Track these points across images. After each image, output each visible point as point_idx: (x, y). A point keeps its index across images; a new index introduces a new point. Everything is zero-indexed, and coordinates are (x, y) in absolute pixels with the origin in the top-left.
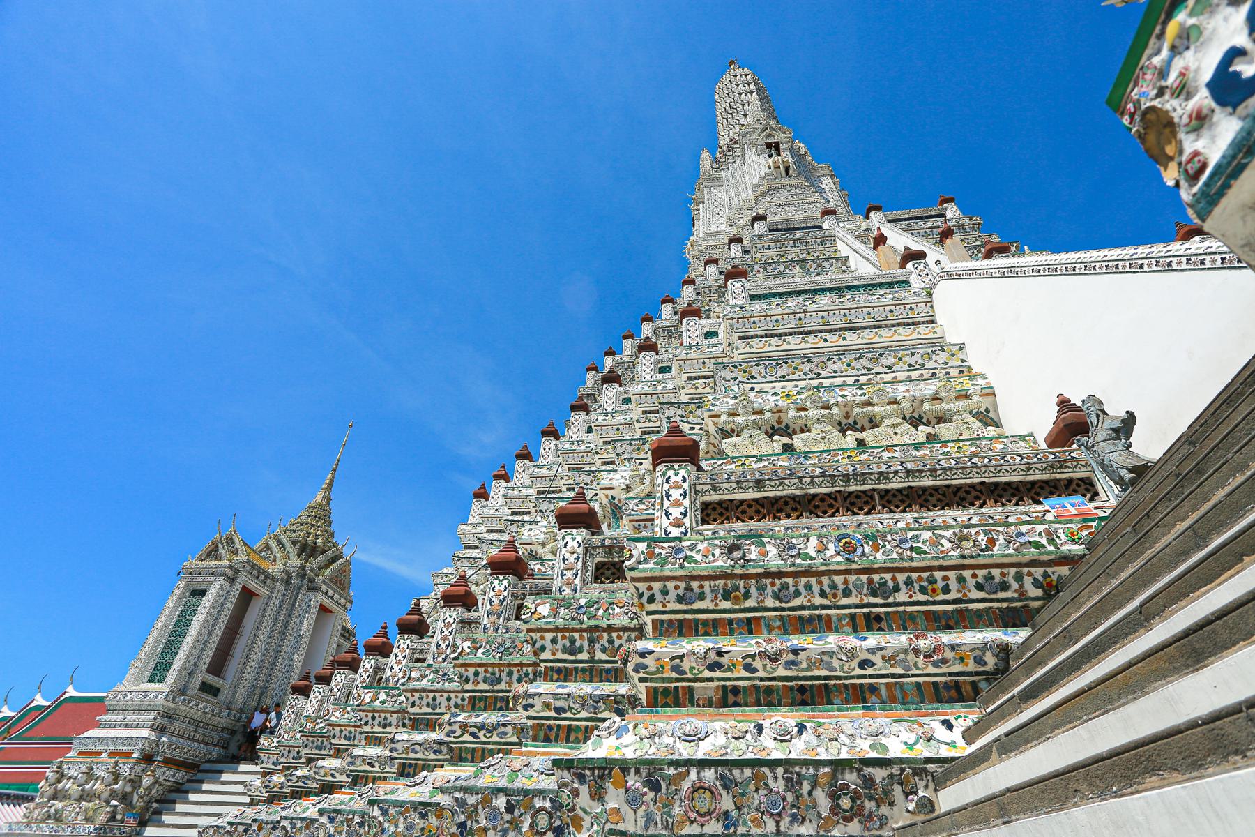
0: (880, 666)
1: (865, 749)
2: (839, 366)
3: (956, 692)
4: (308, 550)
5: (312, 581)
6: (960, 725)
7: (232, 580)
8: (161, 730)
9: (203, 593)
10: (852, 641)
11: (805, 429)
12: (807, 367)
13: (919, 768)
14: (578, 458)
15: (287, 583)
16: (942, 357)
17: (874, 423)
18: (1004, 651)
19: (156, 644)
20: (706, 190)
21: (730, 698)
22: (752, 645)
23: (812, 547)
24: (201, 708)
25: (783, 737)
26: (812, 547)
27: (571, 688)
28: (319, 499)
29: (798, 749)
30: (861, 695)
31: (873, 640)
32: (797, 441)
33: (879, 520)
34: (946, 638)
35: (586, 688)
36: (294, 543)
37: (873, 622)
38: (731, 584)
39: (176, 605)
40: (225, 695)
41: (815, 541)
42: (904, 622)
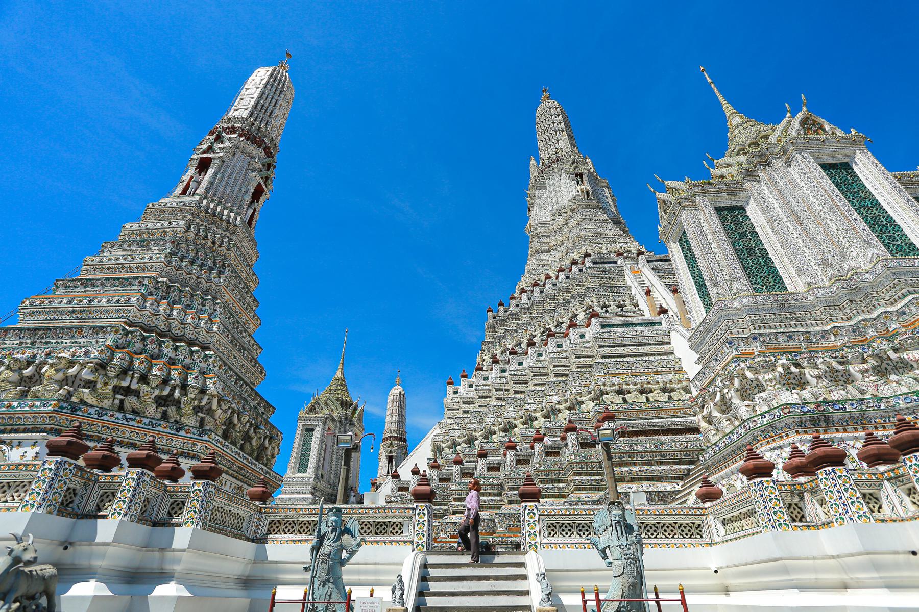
0: (664, 473)
1: (663, 489)
2: (638, 365)
3: (679, 478)
4: (345, 404)
5: (351, 420)
6: (680, 484)
7: (325, 423)
8: (313, 494)
9: (313, 430)
10: (657, 468)
11: (629, 393)
12: (627, 365)
13: (673, 492)
14: (518, 378)
15: (340, 422)
16: (673, 363)
17: (651, 391)
18: (689, 470)
19: (297, 454)
20: (537, 192)
21: (633, 480)
22: (637, 468)
23: (648, 446)
24: (321, 485)
25: (647, 487)
26: (648, 446)
27: (584, 478)
28: (339, 374)
29: (650, 489)
30: (659, 479)
31: (662, 468)
32: (627, 396)
33: (663, 438)
34: (677, 467)
35: (588, 478)
36: (338, 400)
37: (661, 463)
38: (631, 454)
39: (301, 436)
40: (325, 476)
41: (647, 443)
42: (668, 463)
